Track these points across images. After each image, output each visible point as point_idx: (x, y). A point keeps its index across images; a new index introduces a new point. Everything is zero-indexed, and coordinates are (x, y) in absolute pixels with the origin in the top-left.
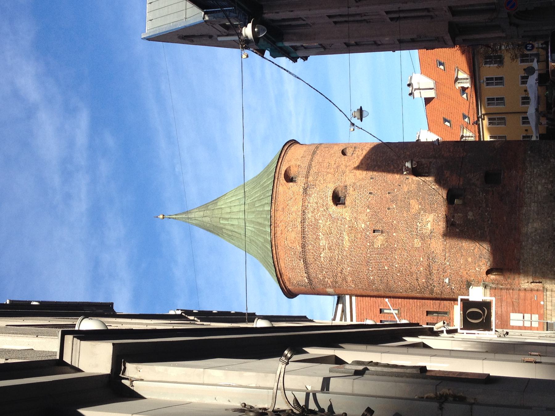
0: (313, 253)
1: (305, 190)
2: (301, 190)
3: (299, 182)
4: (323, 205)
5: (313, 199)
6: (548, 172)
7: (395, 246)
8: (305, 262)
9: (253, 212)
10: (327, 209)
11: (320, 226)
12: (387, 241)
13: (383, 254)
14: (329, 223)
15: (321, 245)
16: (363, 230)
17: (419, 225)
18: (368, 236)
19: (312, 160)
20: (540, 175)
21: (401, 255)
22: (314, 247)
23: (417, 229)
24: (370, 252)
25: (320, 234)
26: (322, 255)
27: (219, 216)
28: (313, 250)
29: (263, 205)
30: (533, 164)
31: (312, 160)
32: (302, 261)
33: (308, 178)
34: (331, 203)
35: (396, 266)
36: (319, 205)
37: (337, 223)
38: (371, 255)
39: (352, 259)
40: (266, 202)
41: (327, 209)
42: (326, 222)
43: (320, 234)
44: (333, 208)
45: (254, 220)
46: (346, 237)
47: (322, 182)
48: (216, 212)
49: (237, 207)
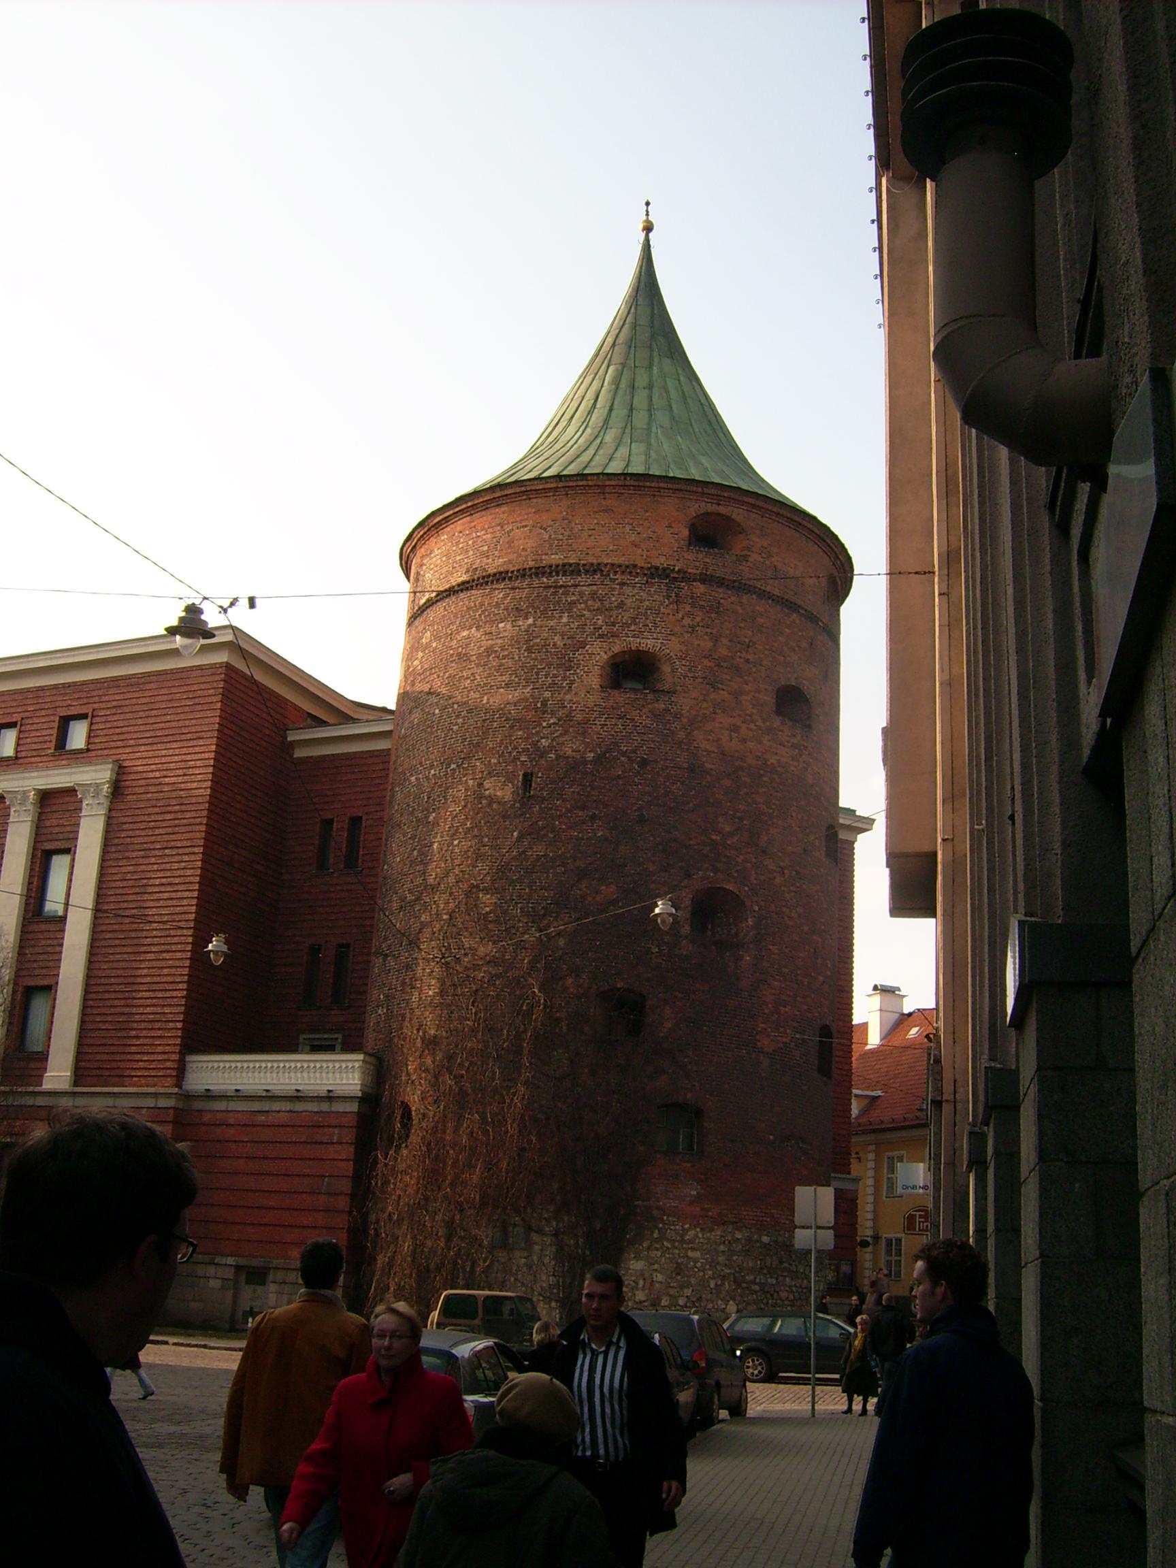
2: (660, 562)
3: (690, 556)
4: (613, 624)
5: (635, 595)
10: (601, 636)
11: (552, 617)
14: (560, 644)
15: (501, 625)
25: (530, 621)
30: (722, 1248)
33: (703, 581)
36: (614, 613)
41: (601, 636)
43: (530, 621)
47: (687, 621)
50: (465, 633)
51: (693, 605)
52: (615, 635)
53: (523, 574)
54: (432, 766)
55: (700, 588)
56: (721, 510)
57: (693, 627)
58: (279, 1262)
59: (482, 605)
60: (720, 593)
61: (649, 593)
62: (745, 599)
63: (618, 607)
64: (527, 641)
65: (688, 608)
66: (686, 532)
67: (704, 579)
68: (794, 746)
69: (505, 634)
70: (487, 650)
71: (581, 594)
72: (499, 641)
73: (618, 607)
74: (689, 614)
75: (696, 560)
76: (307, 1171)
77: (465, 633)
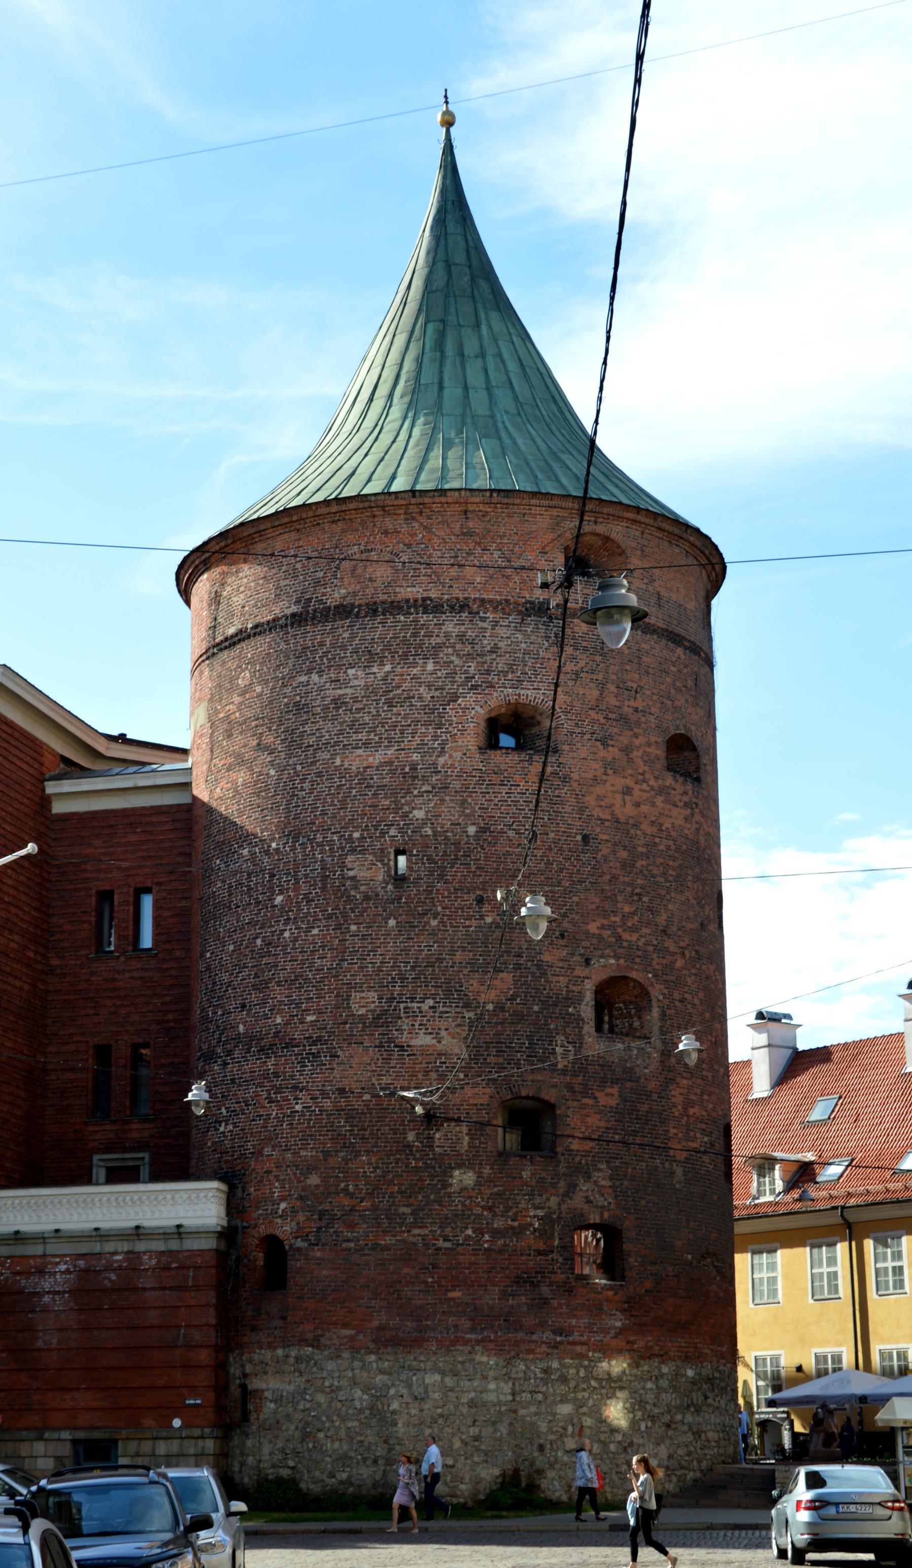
7: (353, 928)
12: (367, 898)
13: (324, 889)
15: (351, 672)
16: (405, 816)
17: (425, 1007)
18: (383, 834)
21: (323, 947)
23: (412, 999)
24: (331, 843)
35: (287, 934)
37: (426, 724)
38: (320, 845)
39: (303, 781)
42: (429, 686)
44: (475, 710)
46: (377, 758)
69: (356, 683)
72: (349, 691)
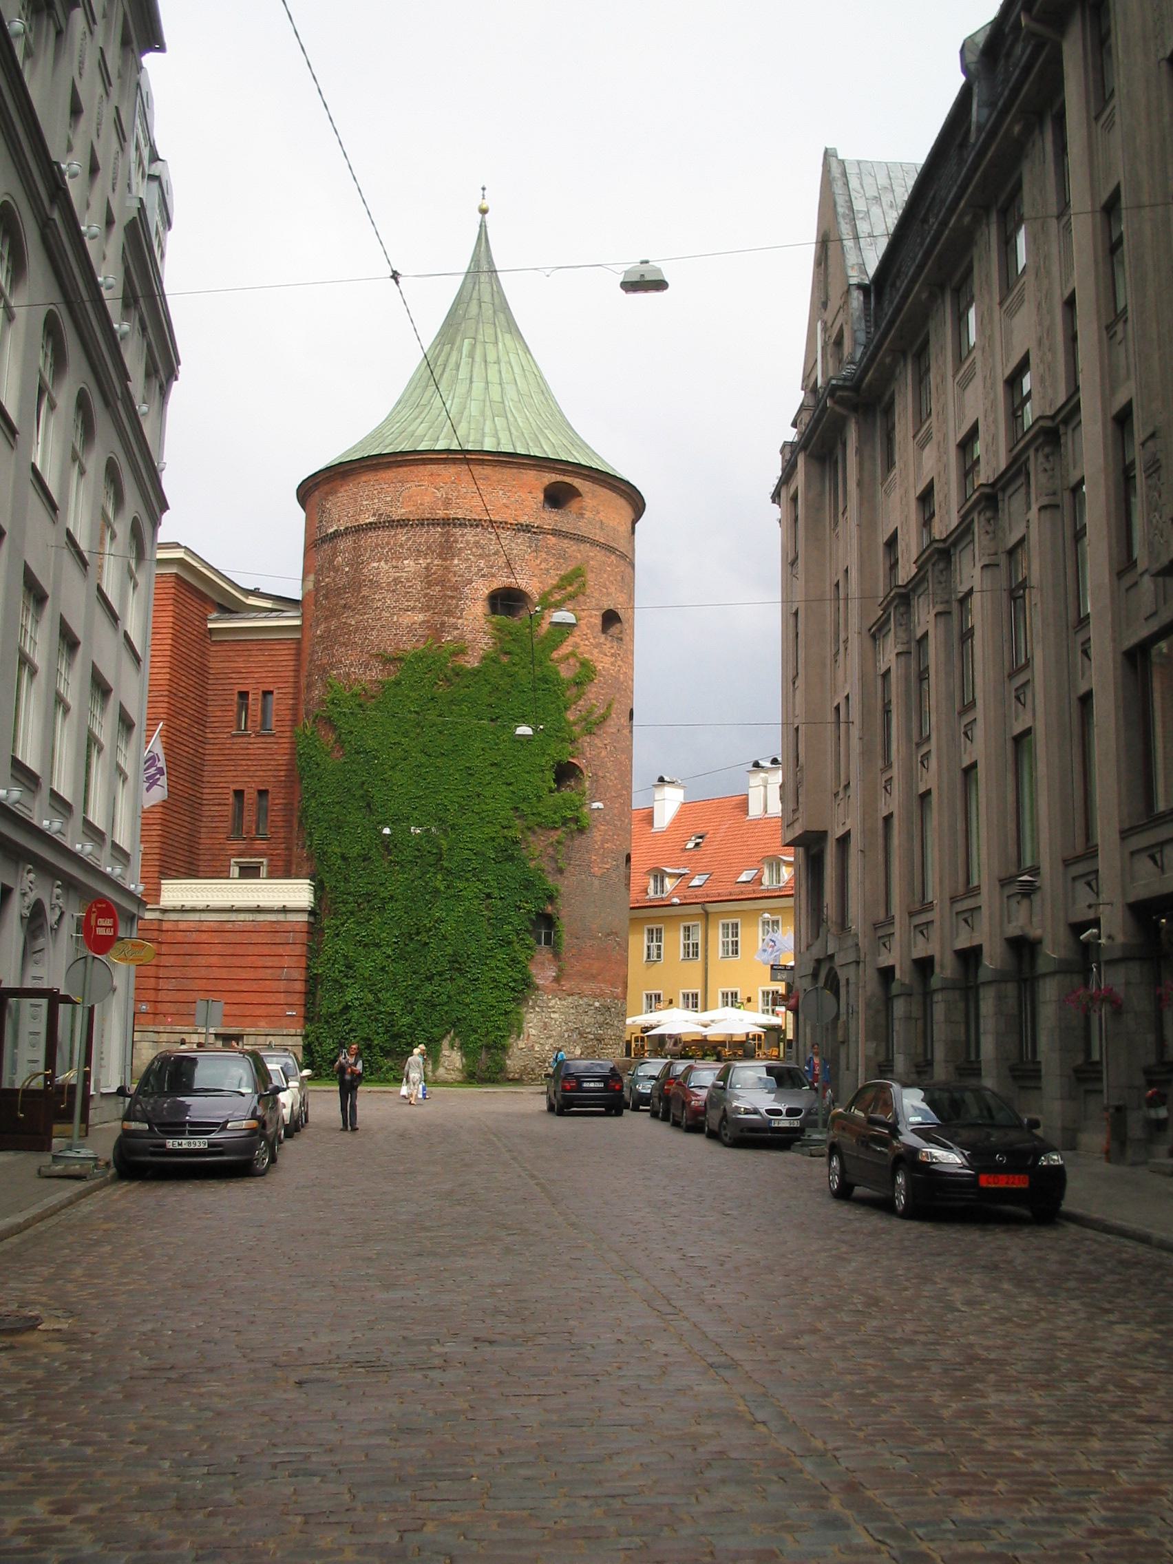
0: (388, 543)
1: (526, 528)
2: (524, 520)
3: (545, 515)
6: (551, 1041)
8: (371, 527)
9: (483, 414)
10: (483, 576)
19: (594, 543)
20: (545, 1026)
22: (401, 546)
26: (382, 563)
27: (480, 337)
28: (395, 544)
29: (496, 435)
31: (594, 543)
32: (372, 520)
34: (496, 584)
40: (503, 441)
41: (483, 576)
45: (466, 413)
47: (543, 566)
48: (489, 331)
49: (498, 376)
50: (375, 564)
51: (547, 553)
52: (493, 576)
53: (421, 523)
54: (352, 665)
55: (552, 540)
56: (567, 479)
57: (547, 570)
58: (252, 1030)
59: (388, 543)
60: (566, 543)
61: (517, 544)
62: (582, 546)
63: (495, 554)
64: (427, 576)
65: (544, 555)
66: (541, 497)
67: (555, 532)
68: (612, 655)
70: (395, 580)
71: (468, 542)
73: (495, 554)
74: (546, 560)
75: (550, 518)
76: (270, 964)
77: (375, 564)
